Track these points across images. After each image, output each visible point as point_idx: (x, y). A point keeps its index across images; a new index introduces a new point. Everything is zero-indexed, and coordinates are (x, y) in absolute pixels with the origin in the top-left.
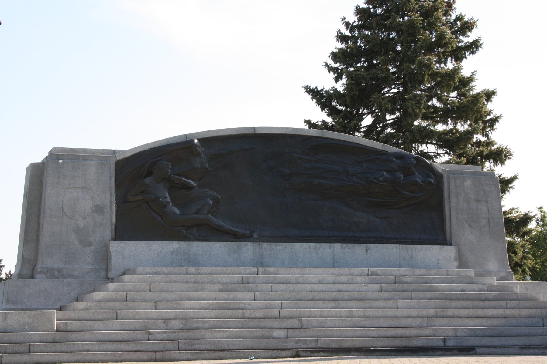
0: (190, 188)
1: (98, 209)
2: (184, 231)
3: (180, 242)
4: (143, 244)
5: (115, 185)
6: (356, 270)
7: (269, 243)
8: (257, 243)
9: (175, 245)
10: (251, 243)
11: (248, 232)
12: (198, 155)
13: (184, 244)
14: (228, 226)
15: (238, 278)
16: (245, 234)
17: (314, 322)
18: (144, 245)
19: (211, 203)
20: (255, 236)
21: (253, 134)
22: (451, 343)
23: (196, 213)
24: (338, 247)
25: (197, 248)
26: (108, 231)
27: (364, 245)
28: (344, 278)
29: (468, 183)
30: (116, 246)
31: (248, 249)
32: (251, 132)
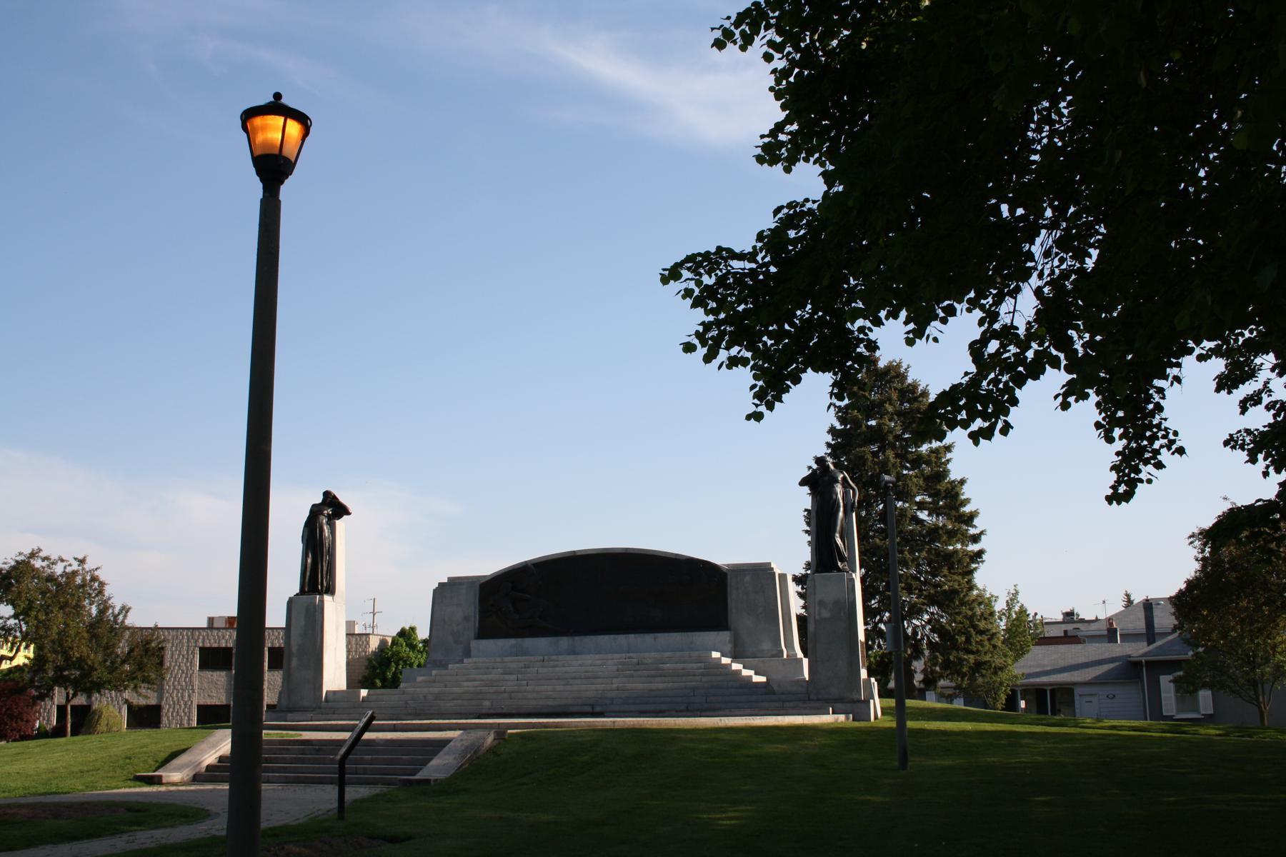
1: (466, 619)
4: (492, 641)
6: (609, 656)
9: (513, 641)
13: (519, 640)
15: (522, 664)
17: (520, 695)
22: (598, 709)
24: (632, 636)
25: (529, 642)
26: (472, 634)
27: (652, 635)
28: (599, 662)
29: (747, 579)
30: (474, 643)
31: (564, 642)
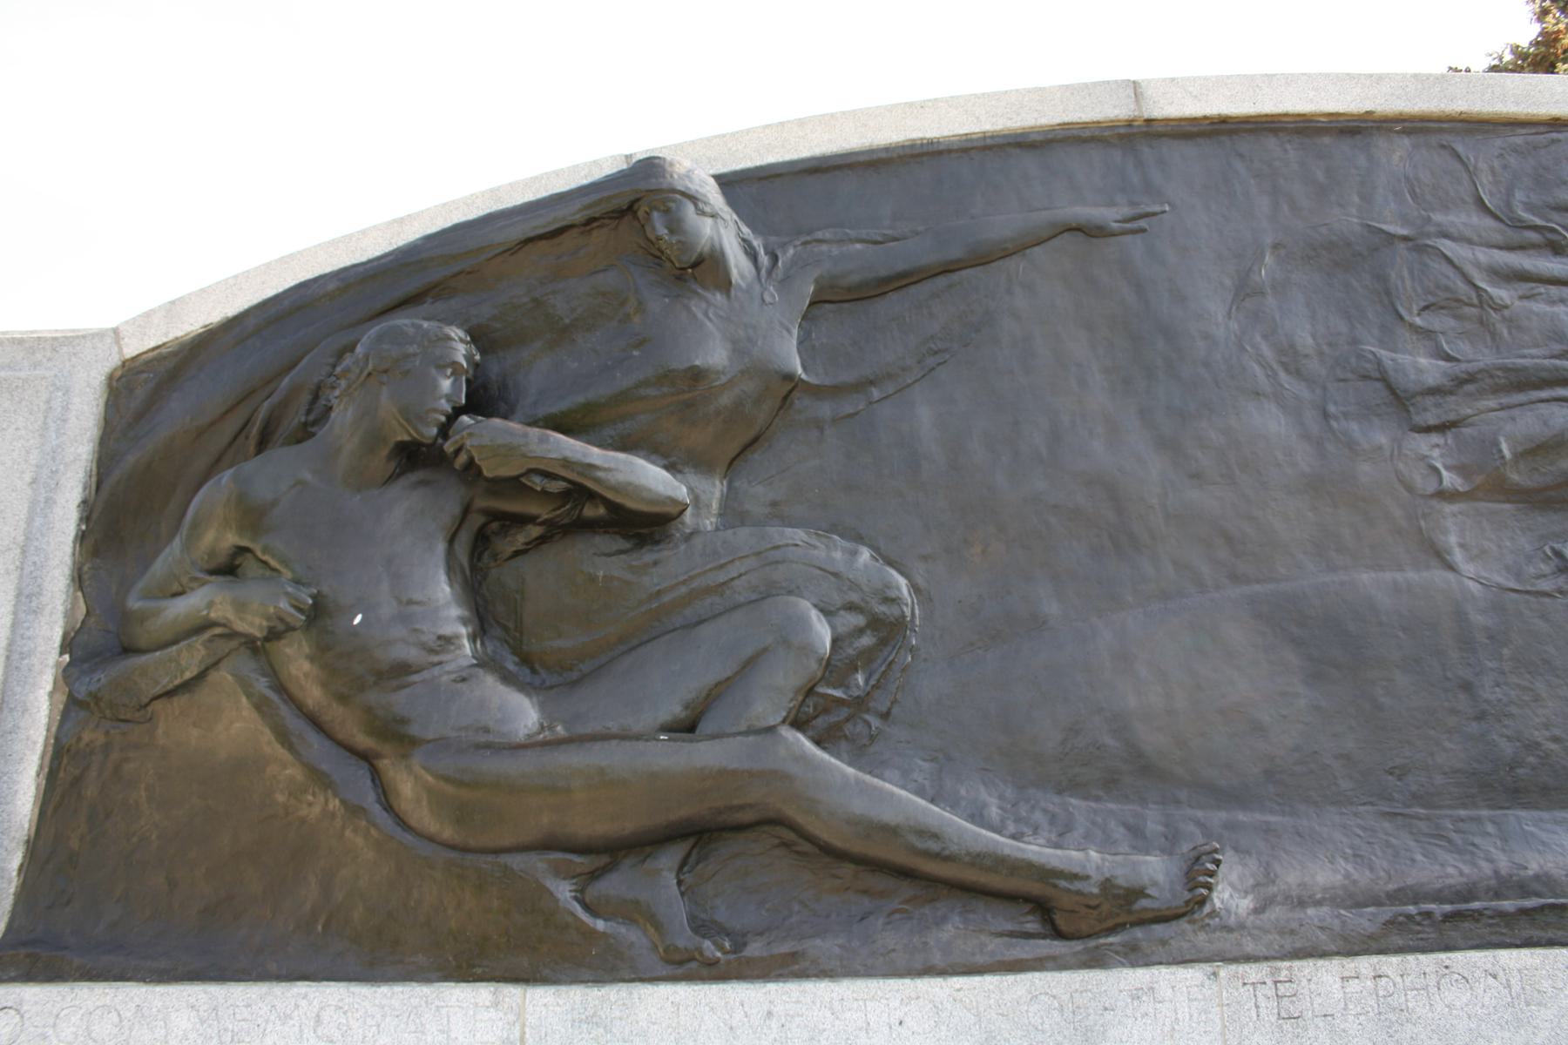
0: (646, 526)
2: (564, 891)
3: (512, 992)
5: (81, 537)
7: (1365, 964)
8: (1253, 972)
10: (1191, 976)
11: (1155, 871)
12: (705, 269)
14: (972, 823)
16: (1139, 893)
18: (183, 1021)
19: (823, 633)
20: (1229, 895)
21: (1129, 123)
23: (687, 727)
32: (1115, 110)
